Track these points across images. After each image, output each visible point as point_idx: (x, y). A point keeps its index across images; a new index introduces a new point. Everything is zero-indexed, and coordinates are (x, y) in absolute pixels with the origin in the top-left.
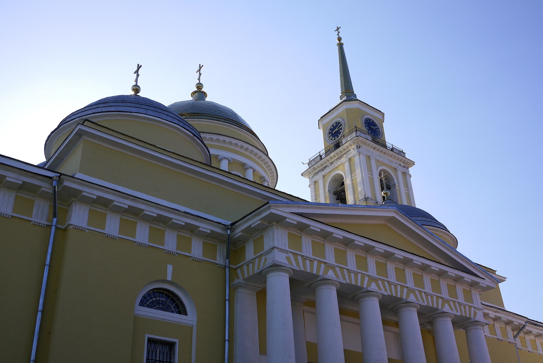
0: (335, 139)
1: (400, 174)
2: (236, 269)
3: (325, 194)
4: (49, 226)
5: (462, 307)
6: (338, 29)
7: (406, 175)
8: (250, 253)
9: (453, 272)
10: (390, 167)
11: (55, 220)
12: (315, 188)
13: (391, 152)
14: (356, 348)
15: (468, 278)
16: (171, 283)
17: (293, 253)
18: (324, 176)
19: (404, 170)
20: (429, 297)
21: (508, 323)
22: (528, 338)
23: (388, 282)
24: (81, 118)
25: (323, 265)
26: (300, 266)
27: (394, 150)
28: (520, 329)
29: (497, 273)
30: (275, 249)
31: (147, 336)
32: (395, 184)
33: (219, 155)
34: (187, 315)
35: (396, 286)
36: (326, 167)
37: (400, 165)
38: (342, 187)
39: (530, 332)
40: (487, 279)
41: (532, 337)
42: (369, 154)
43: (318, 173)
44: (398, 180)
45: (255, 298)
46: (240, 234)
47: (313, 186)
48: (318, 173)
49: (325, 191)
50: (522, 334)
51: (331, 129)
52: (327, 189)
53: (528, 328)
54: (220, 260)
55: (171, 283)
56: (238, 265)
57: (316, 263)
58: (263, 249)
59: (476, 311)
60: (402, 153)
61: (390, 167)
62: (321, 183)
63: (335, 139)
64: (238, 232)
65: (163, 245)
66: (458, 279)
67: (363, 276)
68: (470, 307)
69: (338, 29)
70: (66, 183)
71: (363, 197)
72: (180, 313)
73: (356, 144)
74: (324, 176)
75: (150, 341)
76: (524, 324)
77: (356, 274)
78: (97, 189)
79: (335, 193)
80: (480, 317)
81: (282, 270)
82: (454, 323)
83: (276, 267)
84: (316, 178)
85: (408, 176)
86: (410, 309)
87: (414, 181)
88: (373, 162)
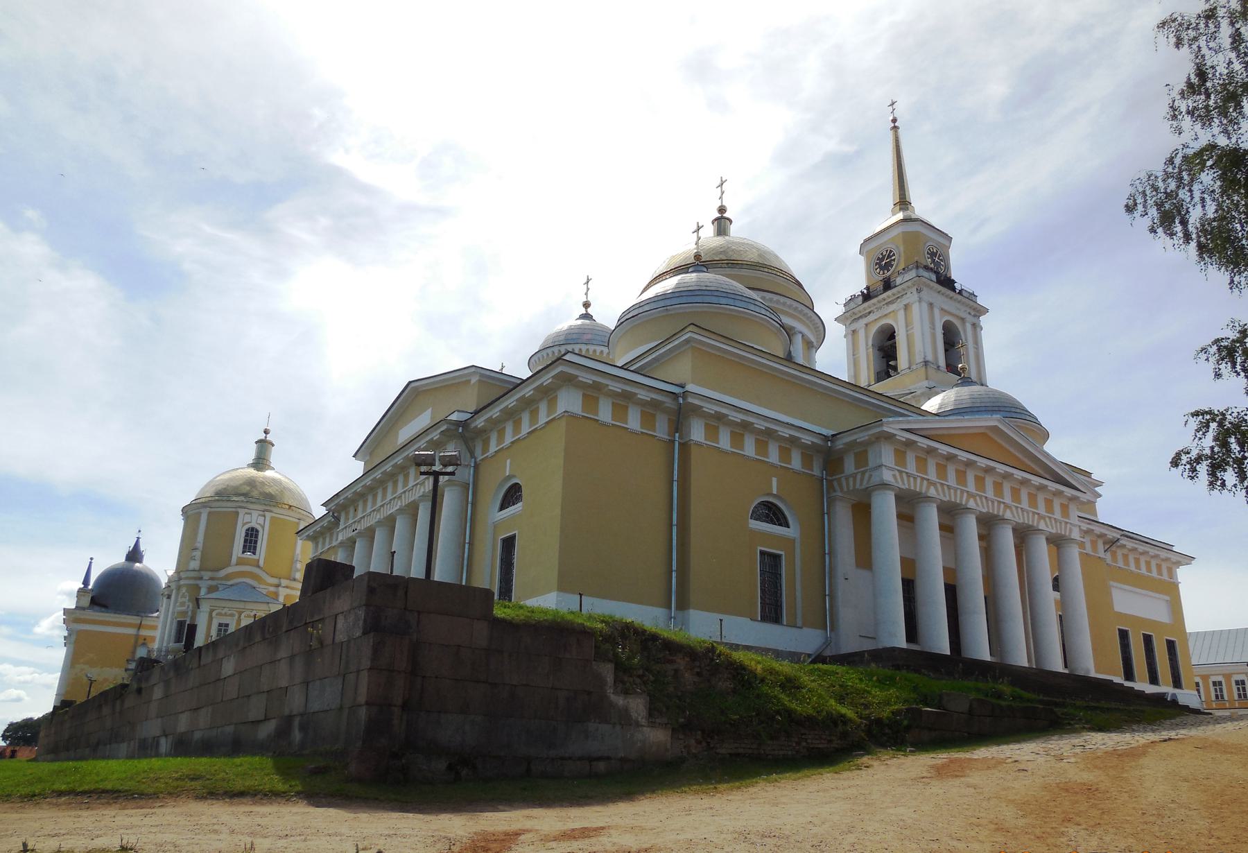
0: (884, 274)
1: (969, 326)
2: (832, 480)
3: (867, 349)
4: (673, 442)
5: (1058, 524)
7: (976, 327)
8: (849, 465)
9: (1053, 486)
10: (957, 317)
11: (677, 435)
13: (959, 297)
14: (952, 565)
15: (1068, 492)
16: (775, 496)
17: (898, 470)
18: (866, 325)
19: (974, 320)
20: (1025, 513)
21: (1101, 536)
22: (1120, 553)
23: (986, 497)
24: (665, 308)
25: (925, 482)
26: (904, 484)
27: (964, 292)
28: (1111, 544)
29: (1093, 476)
30: (884, 468)
31: (760, 548)
34: (789, 527)
35: (993, 502)
36: (870, 313)
37: (969, 313)
38: (890, 342)
39: (1124, 546)
40: (1088, 494)
41: (1125, 551)
42: (931, 300)
44: (966, 334)
45: (850, 514)
46: (841, 446)
47: (850, 337)
48: (859, 318)
49: (867, 345)
50: (1114, 548)
51: (878, 259)
52: (870, 343)
53: (1124, 541)
54: (817, 472)
55: (775, 496)
56: (834, 477)
57: (919, 480)
58: (867, 464)
59: (1073, 527)
60: (973, 296)
61: (957, 317)
63: (884, 274)
64: (840, 444)
65: (768, 458)
66: (1058, 494)
67: (962, 491)
68: (1066, 523)
70: (690, 400)
71: (922, 360)
72: (780, 525)
73: (916, 287)
74: (866, 325)
75: (761, 551)
76: (1119, 537)
77: (956, 490)
78: (714, 404)
80: (1076, 535)
81: (889, 489)
82: (1047, 539)
83: (884, 486)
84: (855, 326)
85: (978, 329)
86: (1006, 526)
88: (937, 311)
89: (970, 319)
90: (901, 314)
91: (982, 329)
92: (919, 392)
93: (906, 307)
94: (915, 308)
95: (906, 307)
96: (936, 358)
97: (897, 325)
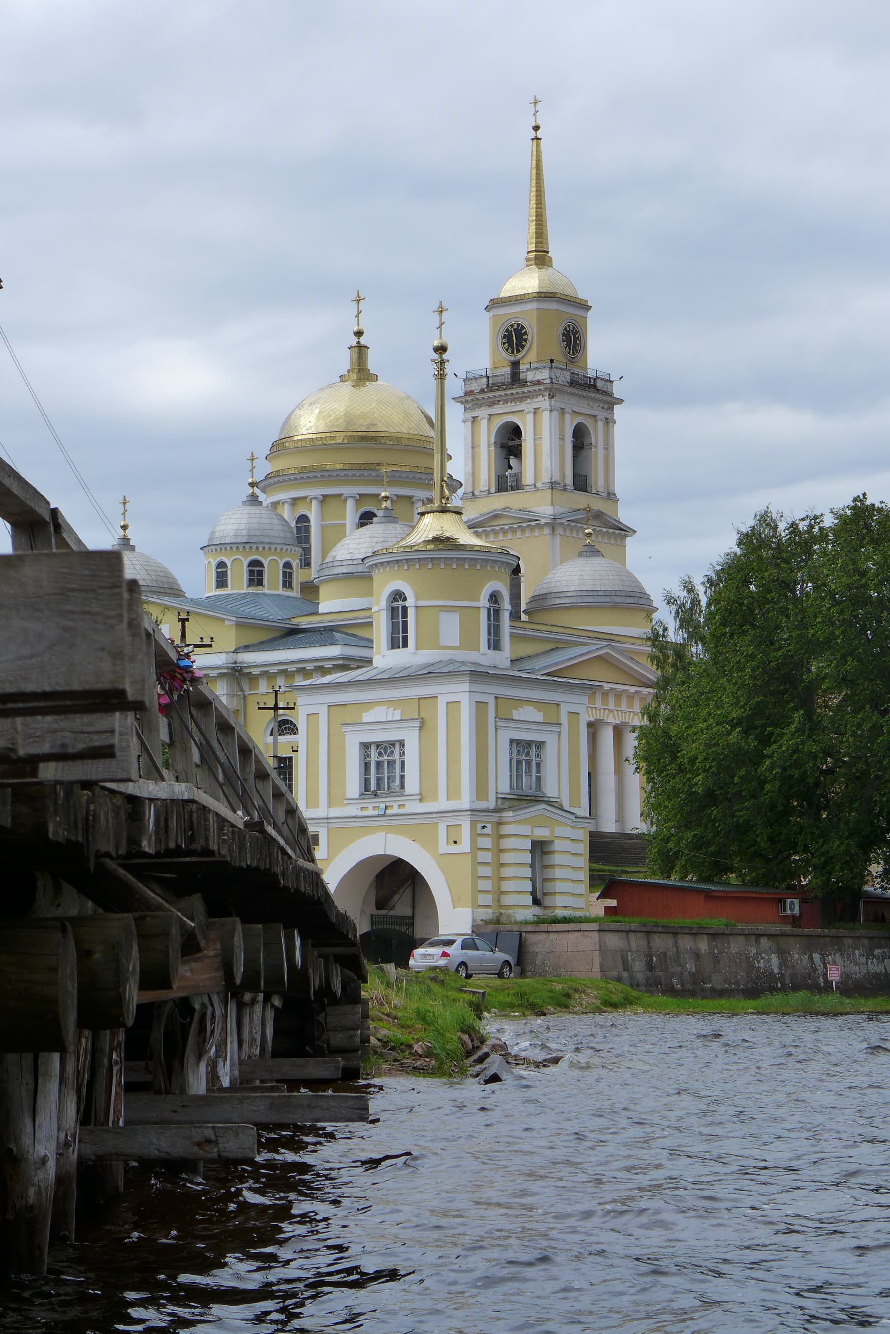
3: (489, 446)
6: (536, 103)
7: (609, 422)
12: (473, 428)
27: (598, 381)
32: (591, 444)
33: (414, 496)
43: (481, 406)
44: (596, 435)
49: (489, 440)
52: (493, 440)
62: (483, 424)
69: (536, 103)
71: (549, 480)
79: (503, 446)
84: (476, 413)
87: (618, 430)
89: (601, 414)
90: (530, 417)
91: (615, 423)
92: (543, 521)
93: (536, 411)
94: (546, 415)
95: (536, 411)
96: (563, 476)
97: (524, 426)
